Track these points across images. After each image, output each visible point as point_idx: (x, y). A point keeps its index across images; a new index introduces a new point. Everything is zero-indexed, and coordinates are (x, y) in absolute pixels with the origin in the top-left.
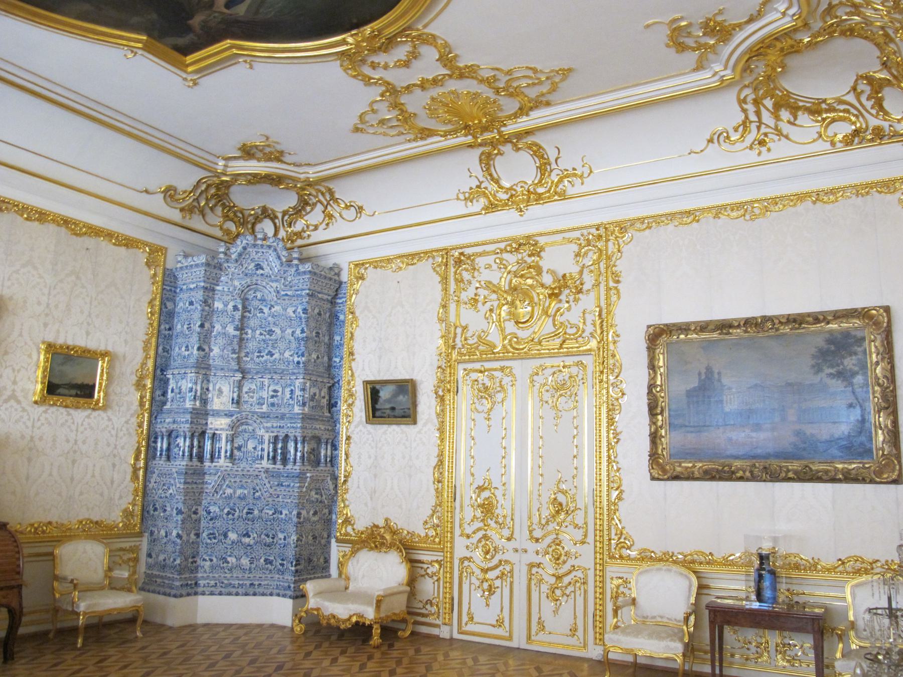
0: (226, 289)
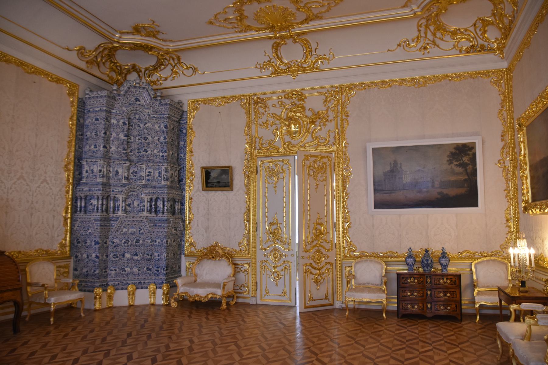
0: (118, 112)
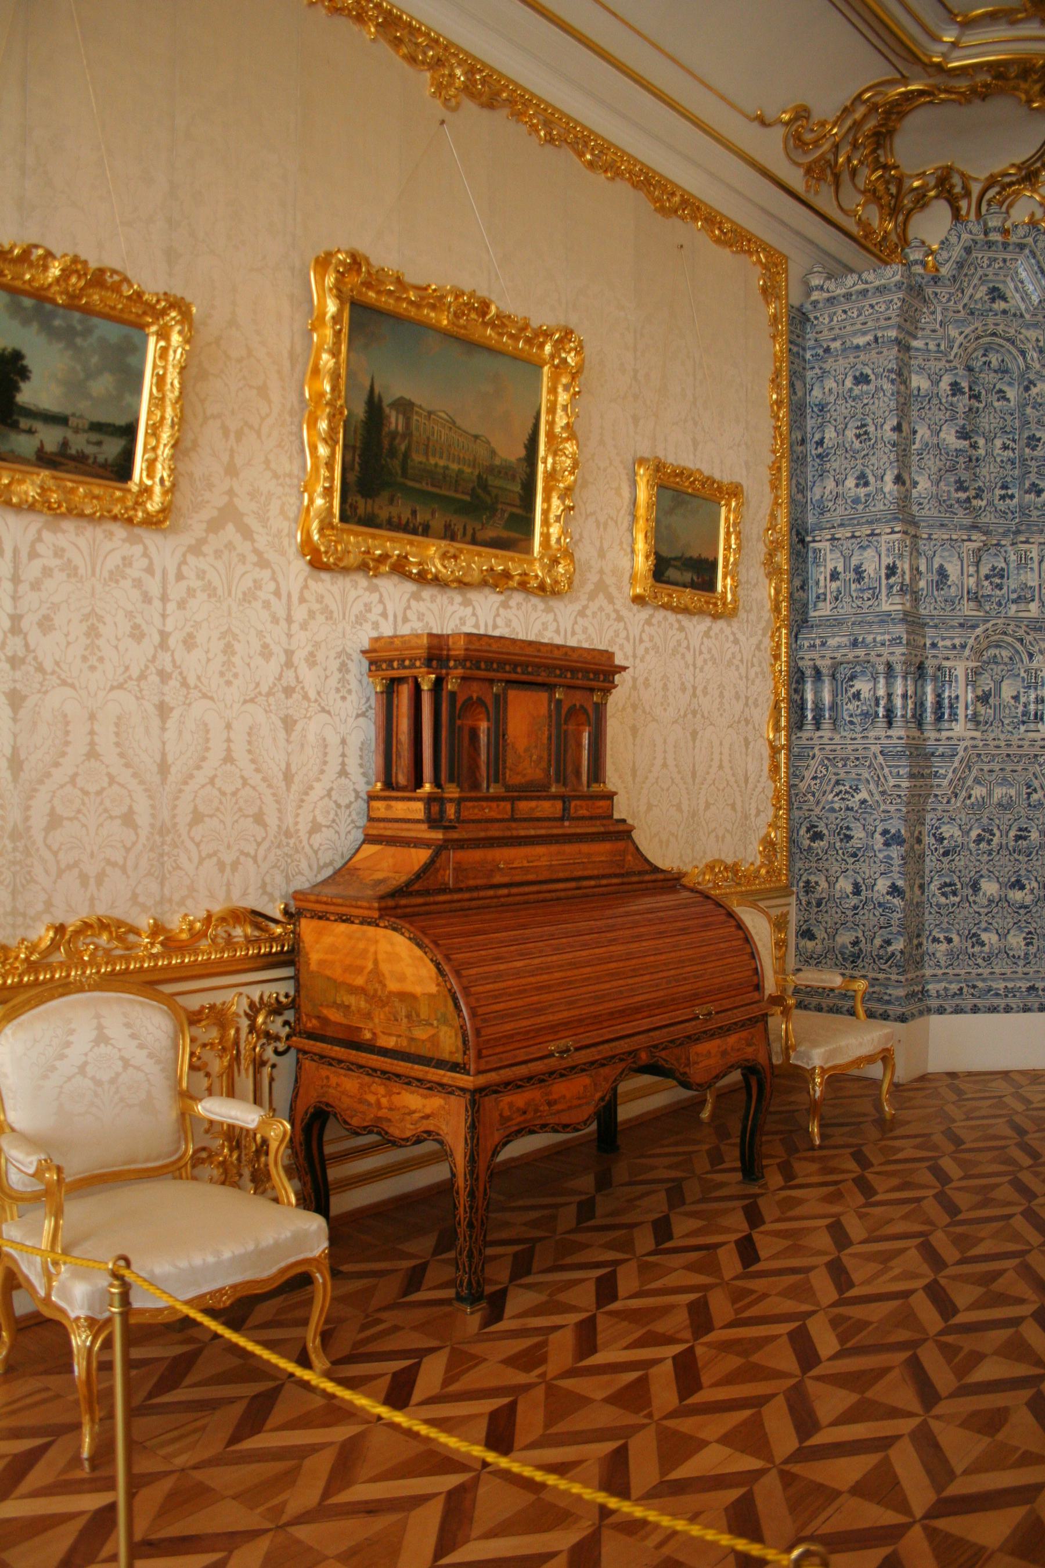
0: (932, 346)
